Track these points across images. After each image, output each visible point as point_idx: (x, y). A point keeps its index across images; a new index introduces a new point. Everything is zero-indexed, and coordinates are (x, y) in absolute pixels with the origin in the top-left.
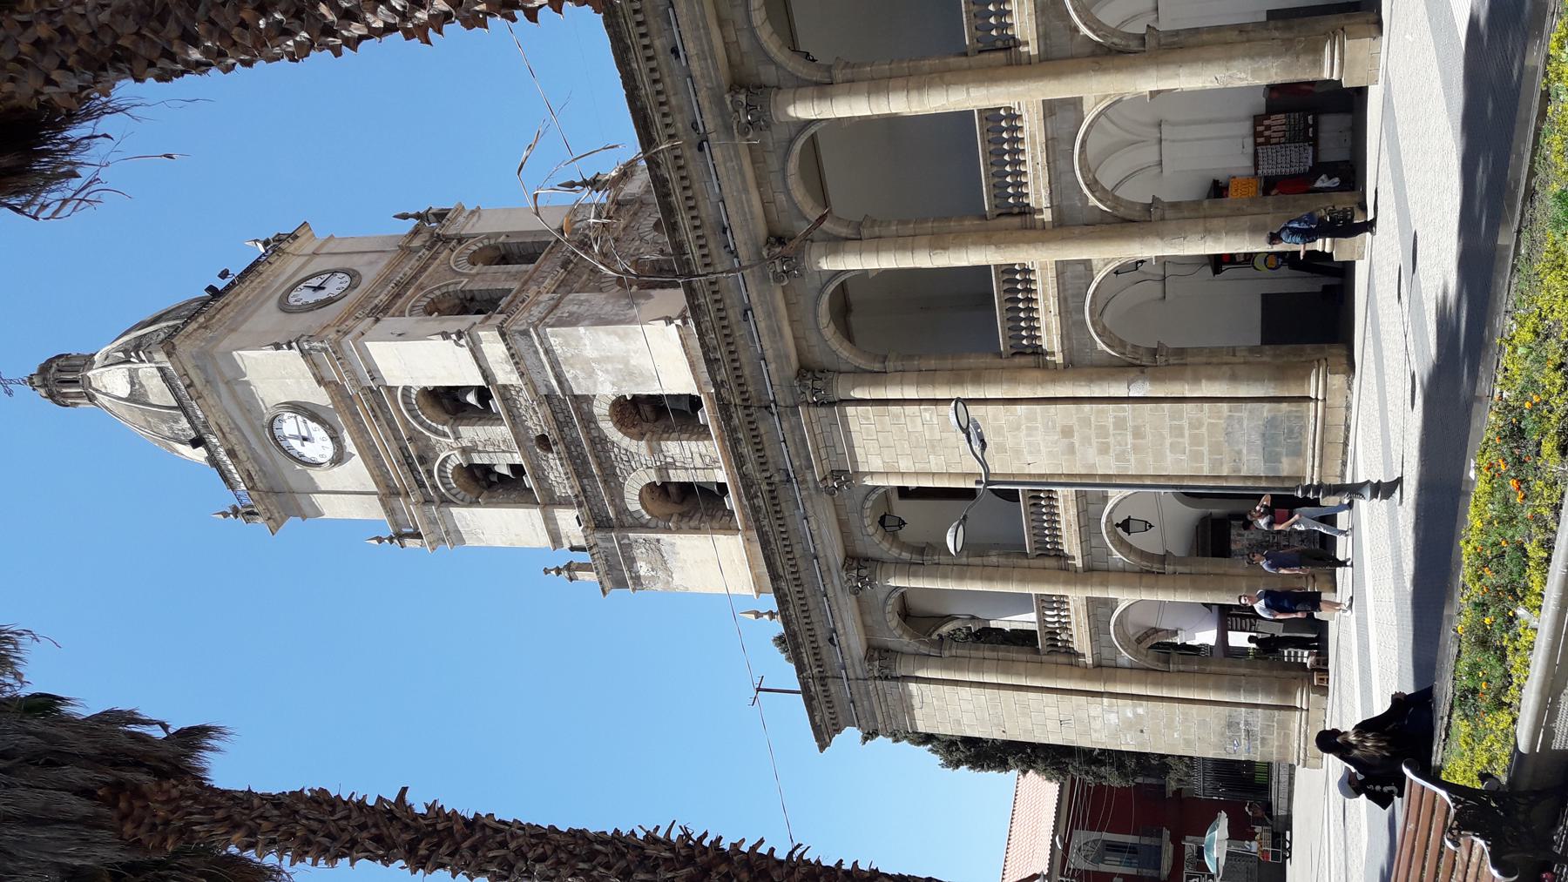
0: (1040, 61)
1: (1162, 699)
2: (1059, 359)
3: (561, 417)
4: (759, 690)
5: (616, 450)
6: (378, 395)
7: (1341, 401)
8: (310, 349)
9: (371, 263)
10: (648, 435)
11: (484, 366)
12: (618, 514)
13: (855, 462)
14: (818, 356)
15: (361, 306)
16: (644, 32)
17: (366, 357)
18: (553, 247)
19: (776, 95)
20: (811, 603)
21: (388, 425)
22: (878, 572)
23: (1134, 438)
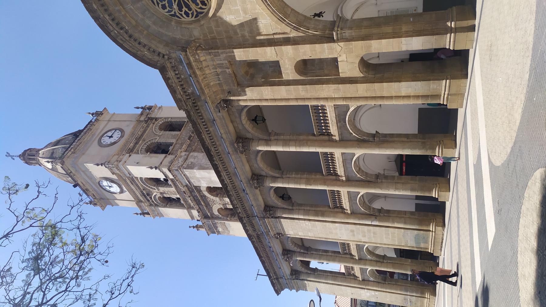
1: (384, 291)
3: (191, 190)
6: (133, 180)
7: (440, 233)
8: (109, 167)
9: (128, 126)
10: (219, 195)
13: (284, 232)
14: (270, 203)
17: (127, 170)
18: (186, 124)
20: (272, 261)
22: (293, 256)
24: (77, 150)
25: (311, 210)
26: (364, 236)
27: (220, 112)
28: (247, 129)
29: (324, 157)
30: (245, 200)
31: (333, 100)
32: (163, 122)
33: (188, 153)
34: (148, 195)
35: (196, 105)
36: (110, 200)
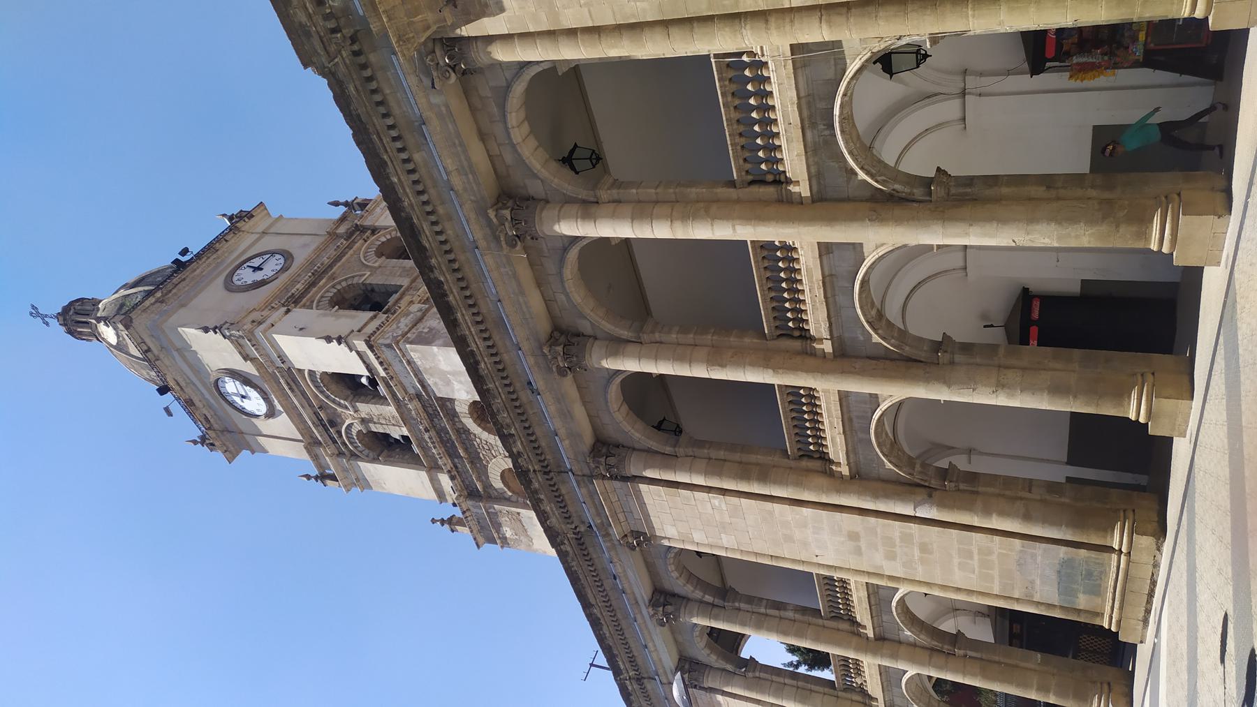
0: (813, 201)
2: (845, 470)
3: (430, 410)
4: (592, 665)
5: (477, 440)
6: (292, 375)
8: (231, 335)
9: (305, 246)
11: (368, 362)
12: (485, 488)
13: (651, 527)
14: (611, 432)
15: (276, 297)
16: (401, 147)
17: (275, 345)
19: (542, 210)
20: (624, 624)
21: (303, 395)
22: (682, 610)
23: (920, 553)
24: (170, 294)
25: (729, 461)
26: (891, 556)
27: (433, 87)
28: (527, 161)
29: (765, 268)
30: (534, 413)
31: (788, 20)
32: (389, 237)
33: (427, 306)
34: (333, 423)
35: (362, 59)
36: (245, 435)
